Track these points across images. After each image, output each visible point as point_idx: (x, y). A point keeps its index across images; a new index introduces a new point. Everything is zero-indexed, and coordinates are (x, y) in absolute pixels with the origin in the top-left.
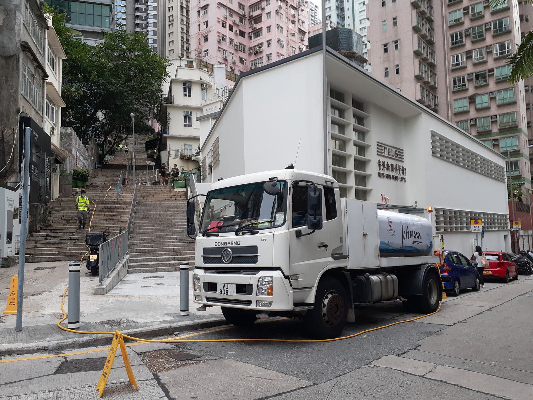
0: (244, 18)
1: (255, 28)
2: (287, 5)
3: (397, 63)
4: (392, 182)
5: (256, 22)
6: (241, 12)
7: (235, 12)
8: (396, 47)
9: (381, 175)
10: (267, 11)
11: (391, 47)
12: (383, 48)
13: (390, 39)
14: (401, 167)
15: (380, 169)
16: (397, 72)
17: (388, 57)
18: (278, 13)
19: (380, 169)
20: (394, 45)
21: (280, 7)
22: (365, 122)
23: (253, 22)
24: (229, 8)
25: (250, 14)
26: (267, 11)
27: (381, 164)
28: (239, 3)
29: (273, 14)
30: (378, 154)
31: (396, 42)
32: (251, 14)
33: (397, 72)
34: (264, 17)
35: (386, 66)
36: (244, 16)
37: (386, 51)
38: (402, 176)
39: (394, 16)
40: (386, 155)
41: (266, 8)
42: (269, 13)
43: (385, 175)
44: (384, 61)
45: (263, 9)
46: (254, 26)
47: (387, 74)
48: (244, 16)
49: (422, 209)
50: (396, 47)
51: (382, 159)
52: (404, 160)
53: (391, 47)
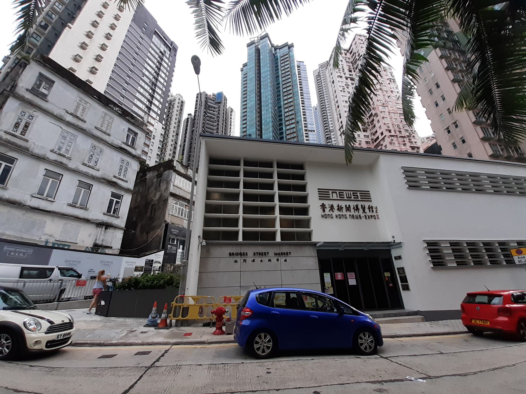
3: (461, 137)
4: (350, 221)
8: (457, 126)
9: (324, 216)
10: (384, 145)
11: (452, 128)
12: (446, 131)
13: (449, 122)
15: (324, 211)
16: (464, 141)
17: (452, 135)
18: (391, 143)
19: (324, 211)
20: (454, 126)
21: (392, 140)
22: (305, 178)
27: (327, 206)
31: (455, 123)
33: (464, 141)
35: (453, 142)
37: (449, 132)
38: (371, 214)
39: (448, 108)
43: (334, 215)
44: (450, 139)
47: (455, 146)
49: (400, 243)
50: (457, 126)
51: (327, 203)
52: (372, 200)
53: (452, 128)
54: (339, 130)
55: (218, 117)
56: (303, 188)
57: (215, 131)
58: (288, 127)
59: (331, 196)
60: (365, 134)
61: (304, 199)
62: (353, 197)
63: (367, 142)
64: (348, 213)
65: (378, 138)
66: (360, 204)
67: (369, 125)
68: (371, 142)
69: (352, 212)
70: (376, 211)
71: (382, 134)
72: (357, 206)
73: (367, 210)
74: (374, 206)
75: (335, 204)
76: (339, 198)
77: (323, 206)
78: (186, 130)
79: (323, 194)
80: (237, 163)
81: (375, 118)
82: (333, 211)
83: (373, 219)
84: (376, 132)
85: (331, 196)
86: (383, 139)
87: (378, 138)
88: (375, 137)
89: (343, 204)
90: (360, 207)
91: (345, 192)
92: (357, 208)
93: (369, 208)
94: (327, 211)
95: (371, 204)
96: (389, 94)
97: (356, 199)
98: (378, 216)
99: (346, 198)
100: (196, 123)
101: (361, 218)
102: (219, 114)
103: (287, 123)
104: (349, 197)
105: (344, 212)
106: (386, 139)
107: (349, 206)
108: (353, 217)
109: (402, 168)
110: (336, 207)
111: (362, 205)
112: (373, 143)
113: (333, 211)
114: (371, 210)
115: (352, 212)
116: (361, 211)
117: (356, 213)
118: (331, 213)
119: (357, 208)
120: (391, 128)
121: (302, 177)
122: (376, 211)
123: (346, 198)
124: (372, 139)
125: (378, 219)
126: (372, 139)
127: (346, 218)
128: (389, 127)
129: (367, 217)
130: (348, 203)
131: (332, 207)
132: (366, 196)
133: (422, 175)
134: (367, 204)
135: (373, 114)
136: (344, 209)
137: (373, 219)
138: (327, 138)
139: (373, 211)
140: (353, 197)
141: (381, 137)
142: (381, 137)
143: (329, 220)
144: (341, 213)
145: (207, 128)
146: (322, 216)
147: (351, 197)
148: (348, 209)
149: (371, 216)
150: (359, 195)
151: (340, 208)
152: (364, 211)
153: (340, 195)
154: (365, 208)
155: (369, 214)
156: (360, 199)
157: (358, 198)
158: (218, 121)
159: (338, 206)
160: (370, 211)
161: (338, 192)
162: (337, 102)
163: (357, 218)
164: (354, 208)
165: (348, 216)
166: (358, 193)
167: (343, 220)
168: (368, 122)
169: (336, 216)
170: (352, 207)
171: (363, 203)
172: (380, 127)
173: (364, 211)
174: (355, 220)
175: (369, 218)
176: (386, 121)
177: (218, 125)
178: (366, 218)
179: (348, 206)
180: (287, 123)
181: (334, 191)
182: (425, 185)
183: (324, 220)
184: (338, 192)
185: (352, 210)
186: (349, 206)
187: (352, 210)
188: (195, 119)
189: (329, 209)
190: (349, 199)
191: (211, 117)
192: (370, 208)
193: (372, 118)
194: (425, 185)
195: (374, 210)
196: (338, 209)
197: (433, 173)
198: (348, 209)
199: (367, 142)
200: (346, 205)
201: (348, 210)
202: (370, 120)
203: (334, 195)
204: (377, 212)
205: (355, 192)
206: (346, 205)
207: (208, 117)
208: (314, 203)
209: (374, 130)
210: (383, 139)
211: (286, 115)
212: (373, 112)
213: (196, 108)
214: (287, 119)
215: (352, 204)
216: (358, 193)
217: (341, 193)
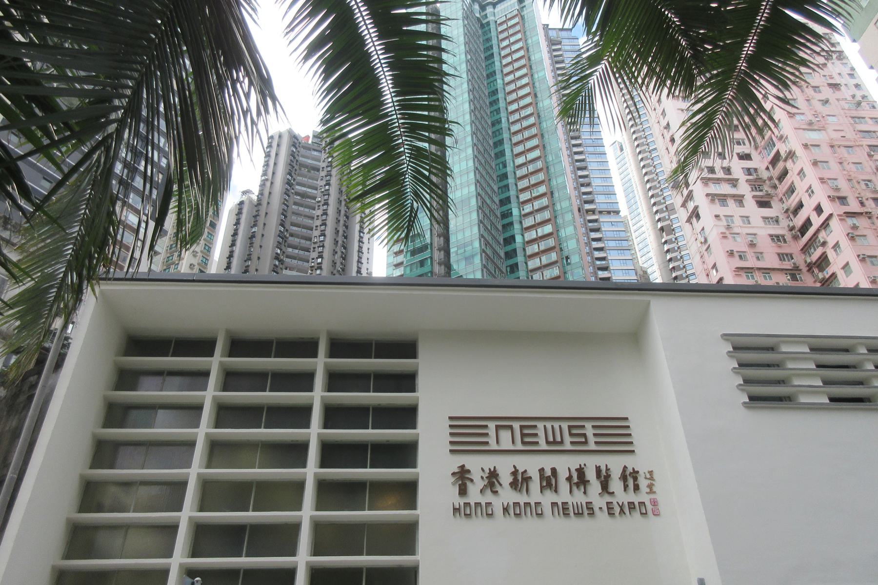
0: (796, 272)
1: (823, 279)
2: (870, 218)
4: (554, 523)
5: (821, 269)
6: (787, 265)
7: (774, 269)
10: (831, 243)
14: (616, 474)
15: (463, 491)
19: (463, 491)
21: (855, 227)
23: (816, 271)
24: (759, 269)
25: (806, 262)
26: (831, 243)
27: (476, 475)
28: (778, 254)
29: (845, 243)
30: (452, 451)
32: (809, 261)
34: (831, 255)
36: (796, 268)
40: (506, 444)
41: (829, 240)
42: (836, 246)
43: (497, 504)
45: (824, 244)
46: (821, 276)
48: (796, 268)
51: (477, 465)
54: (684, 205)
55: (327, 193)
56: (407, 416)
57: (316, 233)
58: (528, 208)
59: (492, 440)
60: (766, 212)
61: (404, 454)
62: (568, 439)
63: (777, 239)
64: (548, 498)
65: (808, 223)
66: (591, 463)
67: (775, 187)
68: (788, 237)
69: (564, 495)
70: (650, 486)
71: (819, 210)
72: (581, 471)
73: (616, 485)
74: (643, 470)
75: (505, 466)
76: (519, 446)
77: (462, 476)
78: (235, 234)
79: (467, 434)
80: (204, 347)
81: (789, 164)
82: (495, 493)
83: (637, 514)
84: (800, 205)
85: (492, 440)
86: (825, 225)
87: (808, 223)
88: (799, 221)
89: (531, 465)
90: (591, 475)
91: (540, 425)
92: (580, 480)
93: (624, 478)
94: (474, 495)
95: (630, 462)
96: (827, 93)
97: (580, 446)
98: (655, 503)
99: (543, 446)
100: (262, 213)
101: (592, 514)
102: (328, 184)
103: (524, 197)
104: (555, 442)
105: (535, 494)
106: (834, 223)
107: (554, 471)
108: (564, 510)
109: (726, 337)
110: (506, 478)
111: (598, 470)
112: (795, 238)
113: (495, 493)
114: (631, 482)
115: (564, 495)
116: (595, 486)
117: (579, 497)
118: (489, 497)
119: (580, 480)
120: (845, 189)
121: (406, 381)
122: (650, 486)
123: (543, 446)
124: (792, 229)
125: (656, 514)
126: (792, 229)
127: (540, 515)
128: (837, 189)
129: (617, 510)
130: (548, 462)
131: (493, 476)
132: (615, 434)
133: (797, 357)
134: (615, 464)
135: (783, 154)
136: (535, 485)
137: (637, 514)
138: (662, 229)
139: (637, 488)
140: (568, 439)
141: (817, 221)
142: (817, 221)
143: (479, 524)
144: (522, 499)
145: (293, 224)
146: (456, 510)
147: (562, 442)
148: (549, 481)
149: (632, 506)
150: (589, 432)
151: (520, 481)
152: (605, 487)
153: (523, 435)
154: (608, 476)
155: (621, 496)
156: (592, 446)
157: (586, 443)
158: (326, 204)
159: (515, 473)
160: (626, 487)
161: (516, 425)
162: (667, 127)
163: (578, 514)
164: (569, 479)
165: (547, 508)
166: (588, 425)
167: (529, 523)
168: (771, 179)
169: (506, 510)
170: (563, 475)
171: (602, 461)
172: (810, 191)
173: (605, 487)
174: (573, 523)
175: (622, 511)
176: (834, 170)
177: (325, 213)
178: (611, 514)
179: (548, 473)
180: (524, 197)
181: (504, 423)
182: (811, 390)
183: (462, 522)
184: (516, 425)
185: (564, 486)
186: (554, 471)
187: (564, 486)
188: (259, 204)
189: (480, 484)
190: (555, 447)
191: (303, 195)
192: (630, 477)
193: (780, 165)
194: (811, 390)
195: (643, 483)
196: (514, 485)
197: (846, 350)
198: (549, 481)
199: (777, 239)
200: (542, 471)
201: (549, 485)
202: (776, 172)
203: (505, 435)
204: (651, 492)
205: (576, 424)
206: (542, 471)
207: (297, 194)
208: (434, 465)
209: (793, 201)
210: (825, 225)
211: (520, 173)
212: (783, 149)
213: (265, 173)
214: (523, 184)
215: (565, 465)
216: (588, 425)
217: (526, 428)
